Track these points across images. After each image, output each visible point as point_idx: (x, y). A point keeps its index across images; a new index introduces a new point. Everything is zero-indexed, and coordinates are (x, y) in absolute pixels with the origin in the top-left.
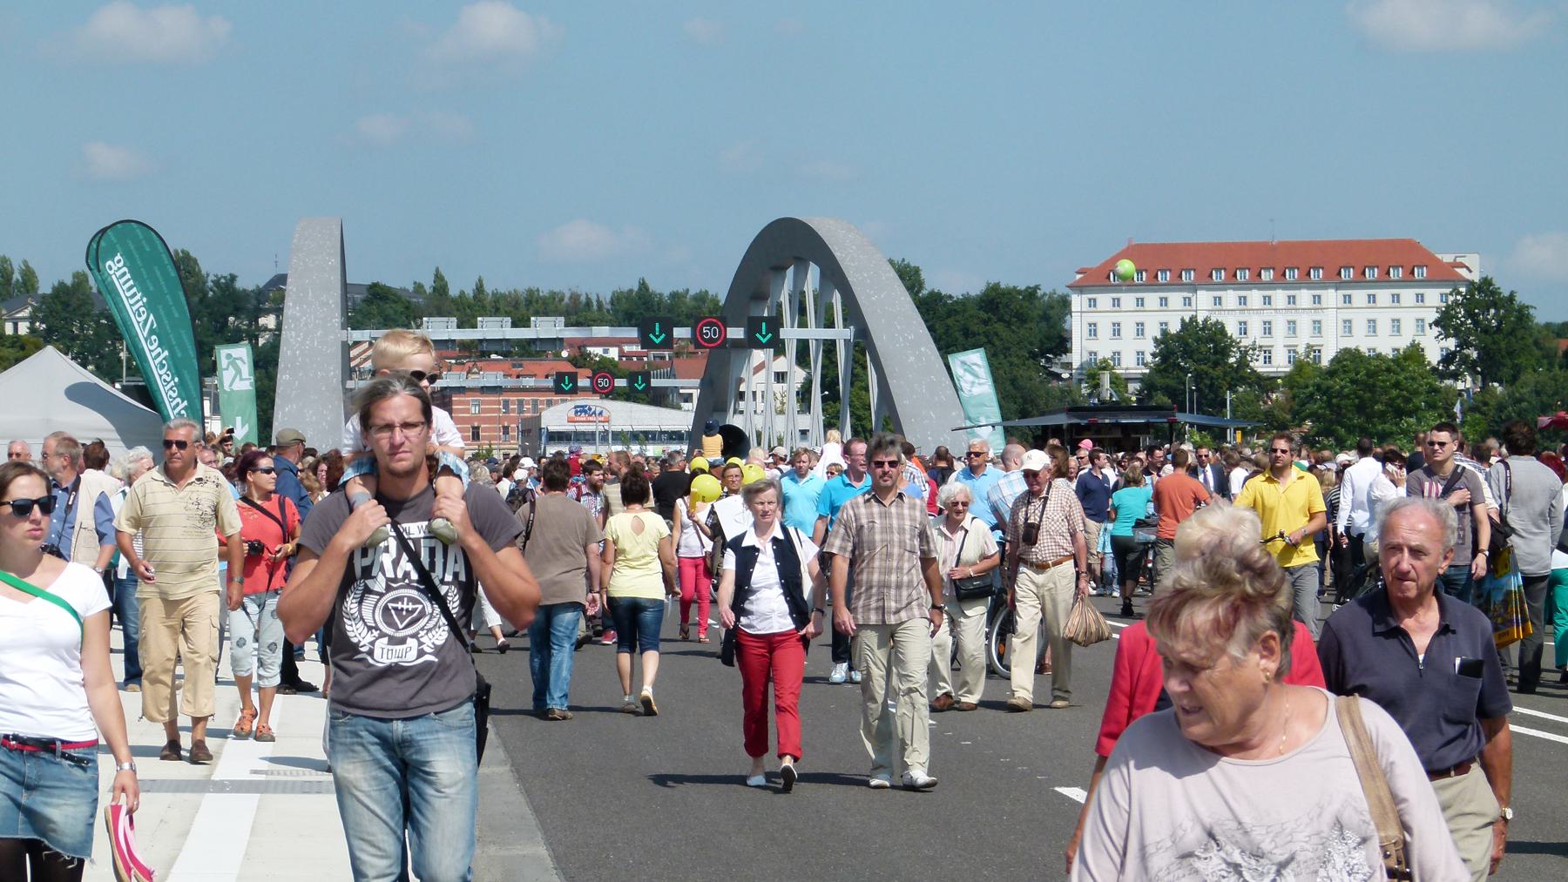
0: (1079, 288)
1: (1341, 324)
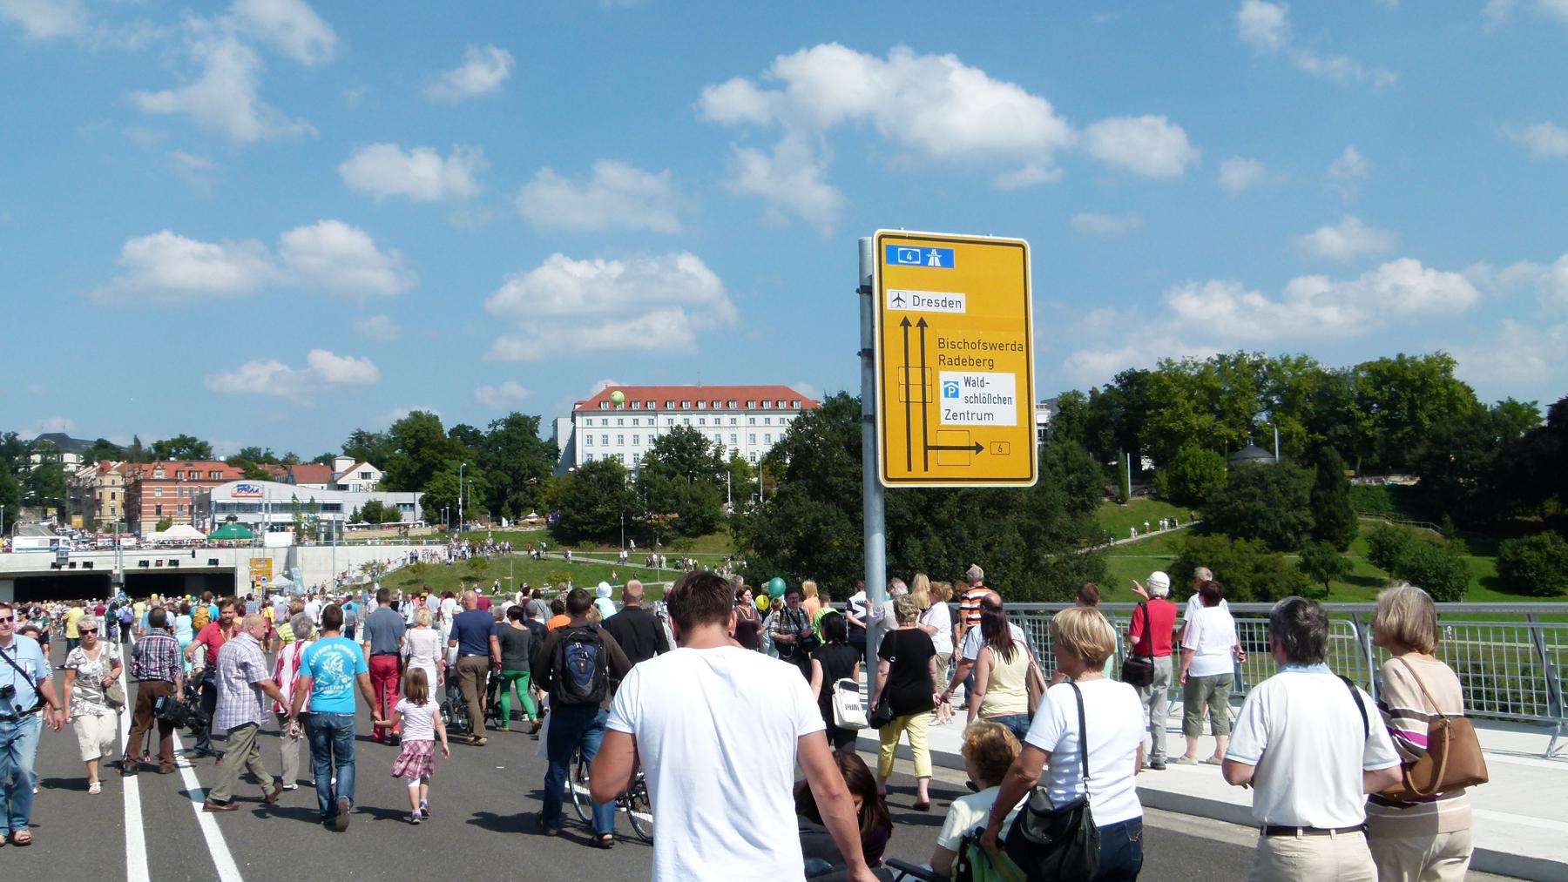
0: (582, 413)
1: (748, 435)
